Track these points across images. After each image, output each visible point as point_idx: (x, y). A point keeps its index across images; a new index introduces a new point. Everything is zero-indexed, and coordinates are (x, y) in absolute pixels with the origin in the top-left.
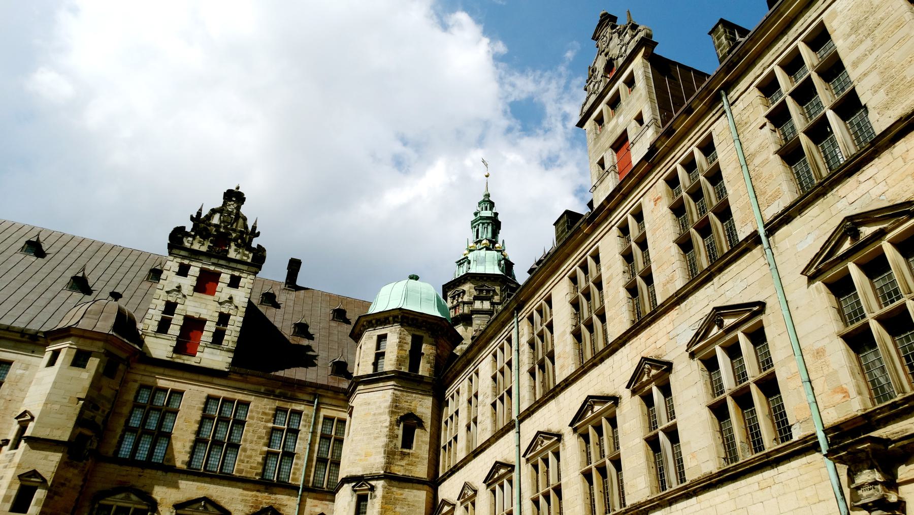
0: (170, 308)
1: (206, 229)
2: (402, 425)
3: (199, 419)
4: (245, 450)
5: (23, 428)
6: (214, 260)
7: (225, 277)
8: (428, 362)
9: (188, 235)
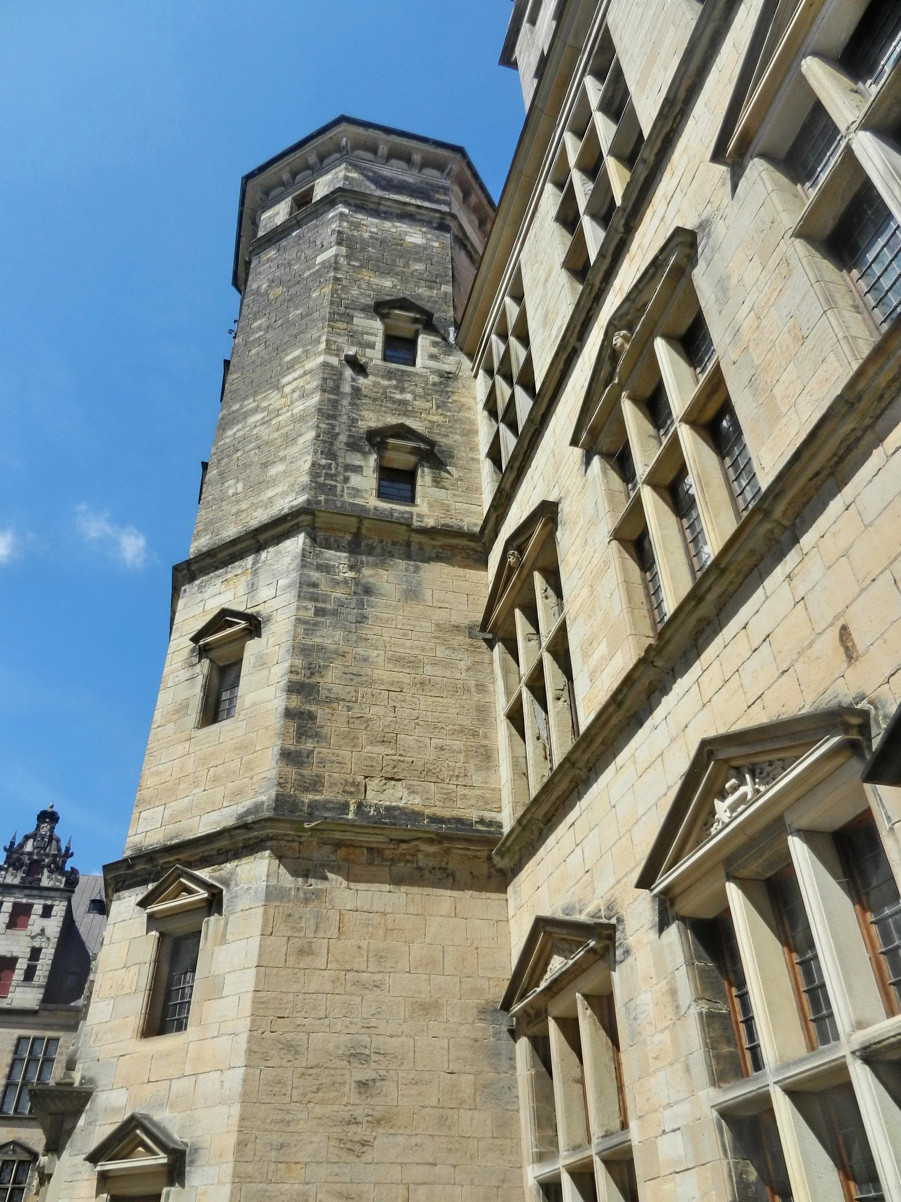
1: (19, 859)
3: (10, 1061)
6: (27, 892)
7: (38, 908)
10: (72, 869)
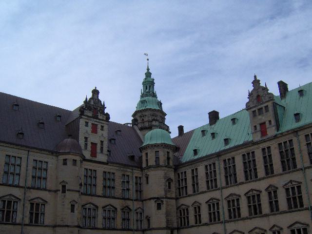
1: (90, 107)
5: (64, 187)
6: (95, 120)
7: (99, 126)
9: (85, 109)
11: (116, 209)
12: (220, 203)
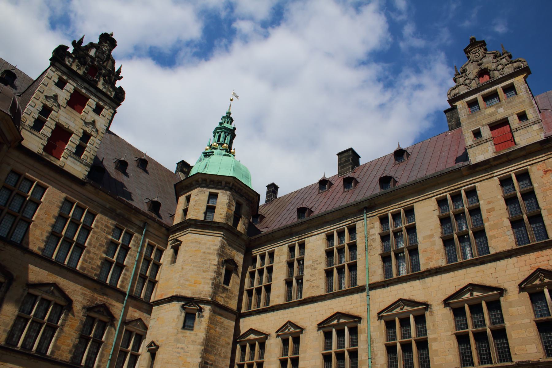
0: (46, 111)
2: (225, 267)
4: (89, 252)
7: (92, 102)
8: (244, 224)
9: (69, 55)
10: (120, 88)
11: (70, 302)
12: (361, 326)
